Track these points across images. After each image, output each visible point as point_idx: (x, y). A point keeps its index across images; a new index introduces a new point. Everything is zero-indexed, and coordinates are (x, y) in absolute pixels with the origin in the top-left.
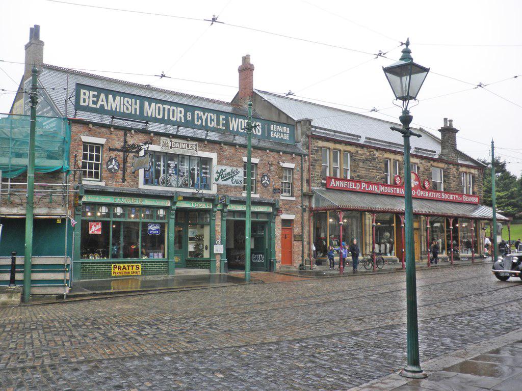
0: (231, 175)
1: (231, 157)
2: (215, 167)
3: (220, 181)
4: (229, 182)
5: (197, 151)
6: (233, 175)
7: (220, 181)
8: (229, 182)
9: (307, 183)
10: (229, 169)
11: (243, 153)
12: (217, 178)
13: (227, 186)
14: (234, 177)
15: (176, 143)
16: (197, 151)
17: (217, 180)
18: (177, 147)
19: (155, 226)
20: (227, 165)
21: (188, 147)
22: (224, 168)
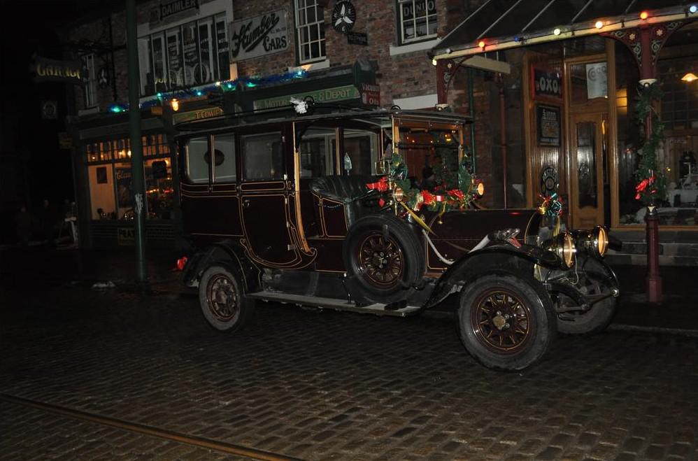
6: (265, 31)
12: (235, 48)
15: (167, 6)
17: (235, 53)
18: (170, 14)
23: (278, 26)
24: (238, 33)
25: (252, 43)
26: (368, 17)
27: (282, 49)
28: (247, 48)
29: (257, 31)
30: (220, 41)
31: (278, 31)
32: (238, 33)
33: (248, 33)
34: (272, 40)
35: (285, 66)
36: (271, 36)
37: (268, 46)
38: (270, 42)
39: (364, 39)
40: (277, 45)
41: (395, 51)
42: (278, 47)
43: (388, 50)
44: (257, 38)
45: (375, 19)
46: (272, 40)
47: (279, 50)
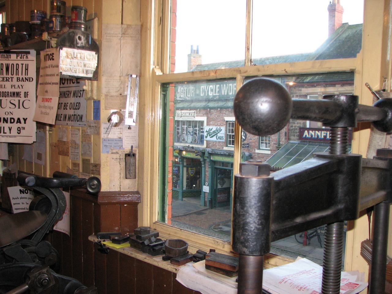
0: (216, 133)
1: (217, 118)
2: (206, 128)
3: (209, 138)
4: (214, 139)
5: (194, 117)
6: (217, 132)
7: (209, 138)
8: (214, 139)
9: (285, 135)
10: (214, 128)
11: (225, 114)
12: (206, 135)
13: (213, 142)
14: (218, 134)
15: (183, 113)
16: (194, 117)
17: (206, 137)
18: (184, 116)
19: (176, 168)
20: (214, 125)
21: (190, 115)
22: (211, 127)
23: (221, 132)
24: (208, 131)
25: (212, 135)
26: (250, 138)
27: (222, 140)
28: (210, 136)
29: (214, 132)
30: (201, 130)
31: (221, 134)
32: (208, 131)
33: (211, 131)
34: (219, 136)
35: (222, 146)
36: (219, 135)
37: (217, 138)
38: (218, 137)
39: (248, 145)
40: (221, 138)
41: (257, 151)
42: (221, 139)
43: (255, 151)
44: (214, 134)
45: (252, 139)
46: (219, 136)
47: (221, 140)
